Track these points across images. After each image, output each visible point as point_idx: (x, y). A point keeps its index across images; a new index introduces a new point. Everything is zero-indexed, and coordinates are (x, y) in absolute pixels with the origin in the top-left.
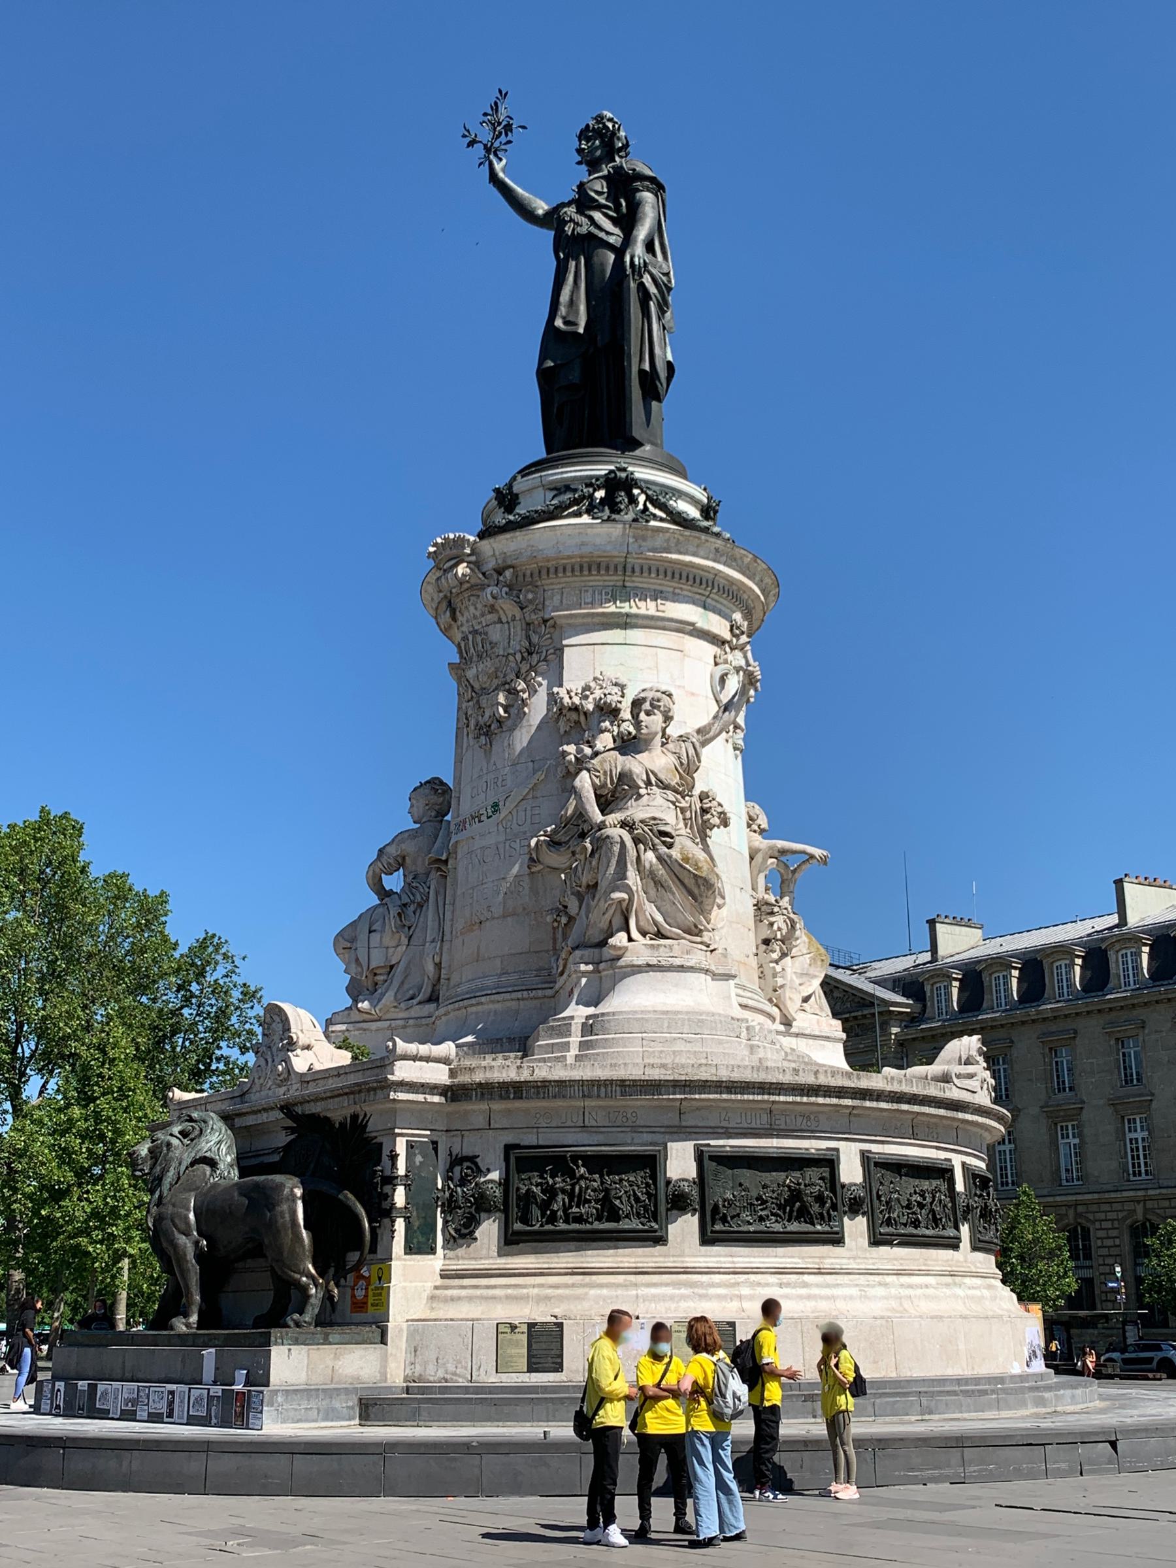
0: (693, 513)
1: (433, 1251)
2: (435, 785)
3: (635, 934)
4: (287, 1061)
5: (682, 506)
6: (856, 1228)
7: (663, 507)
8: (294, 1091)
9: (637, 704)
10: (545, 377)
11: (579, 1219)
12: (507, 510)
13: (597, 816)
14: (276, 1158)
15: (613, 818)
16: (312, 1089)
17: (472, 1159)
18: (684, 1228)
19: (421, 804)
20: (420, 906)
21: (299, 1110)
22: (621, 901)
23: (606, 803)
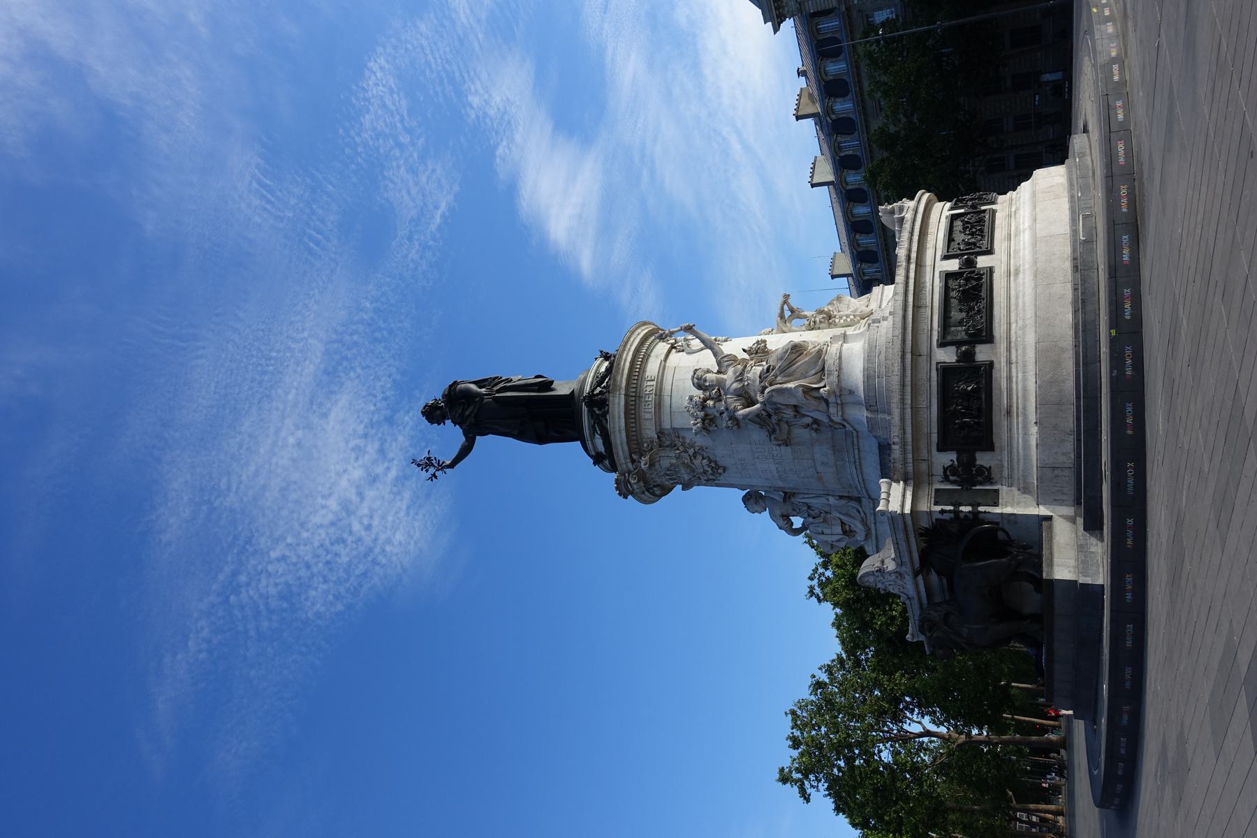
0: (606, 364)
1: (997, 491)
2: (746, 500)
3: (822, 384)
4: (890, 573)
5: (603, 369)
6: (982, 262)
7: (604, 378)
8: (907, 569)
9: (699, 387)
10: (541, 440)
11: (979, 409)
12: (604, 459)
13: (758, 406)
14: (945, 581)
15: (760, 398)
16: (906, 559)
17: (945, 470)
18: (982, 353)
19: (757, 508)
20: (809, 507)
21: (917, 565)
22: (804, 392)
23: (751, 402)
